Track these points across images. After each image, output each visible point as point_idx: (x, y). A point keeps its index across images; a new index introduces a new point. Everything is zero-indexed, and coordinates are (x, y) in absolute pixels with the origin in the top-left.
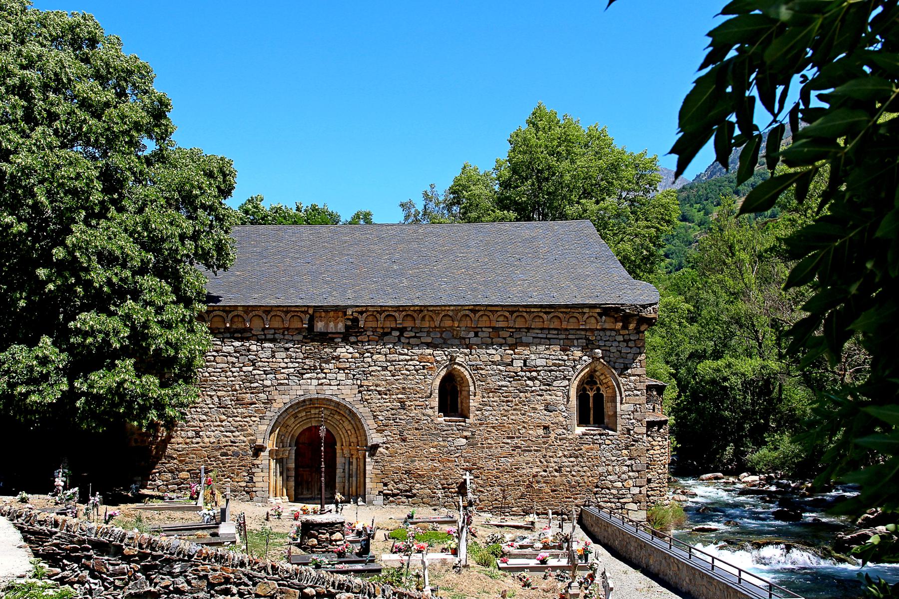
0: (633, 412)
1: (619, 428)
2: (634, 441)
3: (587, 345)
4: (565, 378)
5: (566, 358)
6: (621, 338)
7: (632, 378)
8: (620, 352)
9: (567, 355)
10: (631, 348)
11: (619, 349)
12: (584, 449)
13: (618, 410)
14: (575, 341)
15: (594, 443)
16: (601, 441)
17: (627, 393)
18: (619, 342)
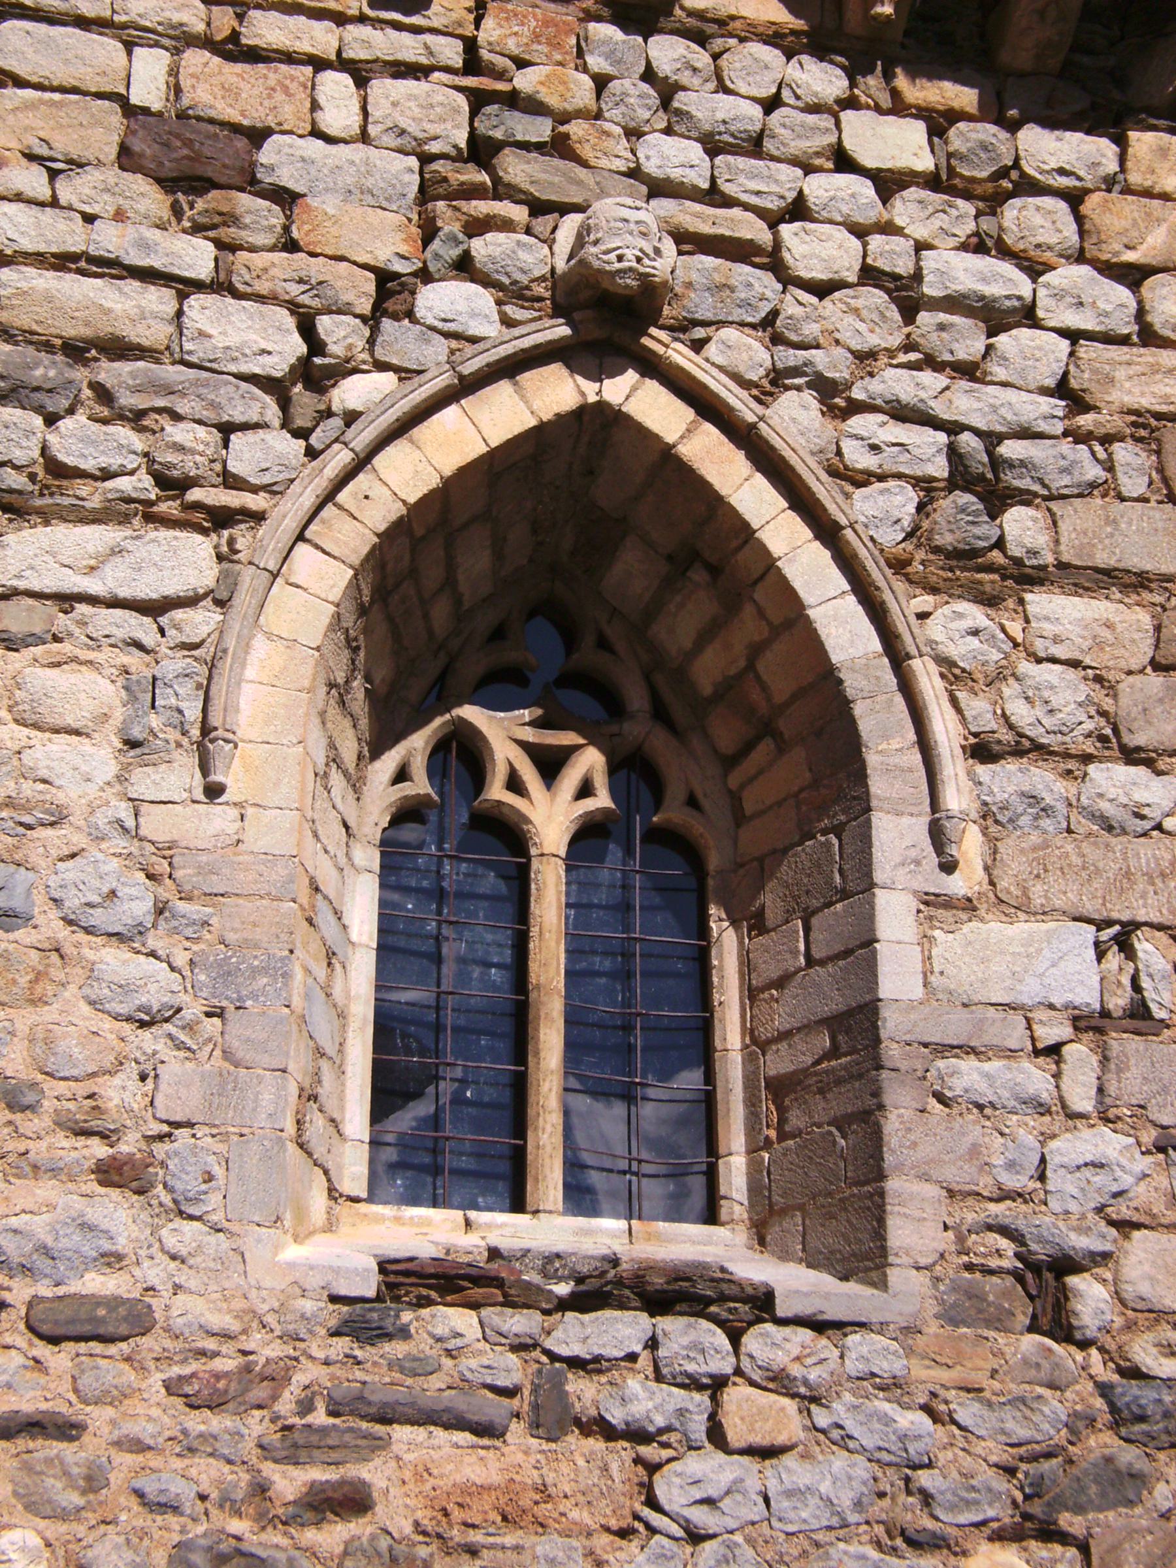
0: (1091, 1023)
1: (916, 1226)
2: (1122, 1418)
3: (481, 151)
4: (169, 499)
5: (196, 257)
6: (902, 144)
7: (1058, 613)
8: (907, 296)
9: (220, 232)
10: (1034, 269)
11: (890, 253)
12: (397, 1512)
13: (897, 979)
14: (336, 84)
15: (554, 1419)
16: (642, 1400)
17: (1007, 779)
18: (888, 184)
